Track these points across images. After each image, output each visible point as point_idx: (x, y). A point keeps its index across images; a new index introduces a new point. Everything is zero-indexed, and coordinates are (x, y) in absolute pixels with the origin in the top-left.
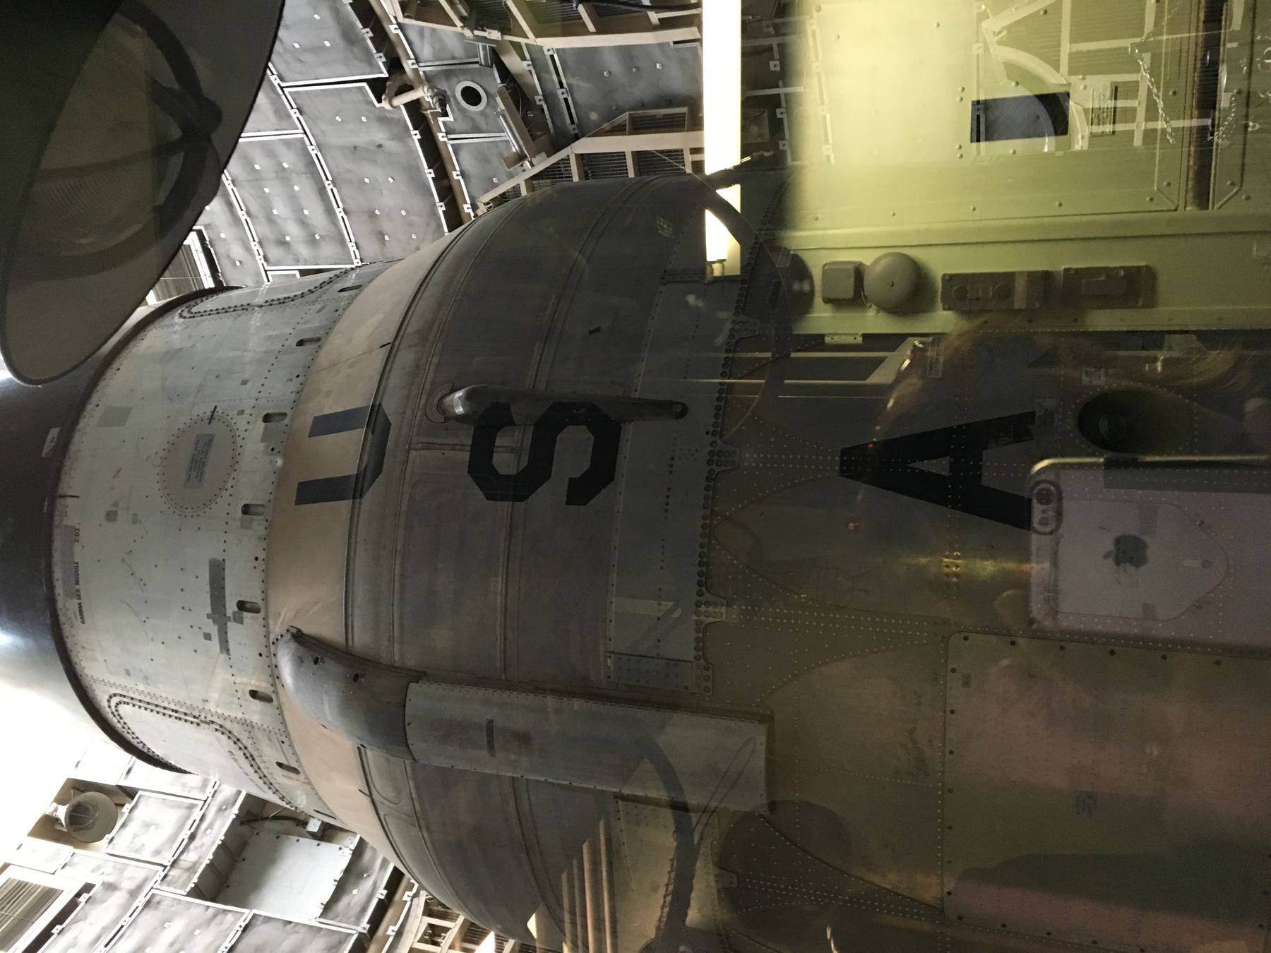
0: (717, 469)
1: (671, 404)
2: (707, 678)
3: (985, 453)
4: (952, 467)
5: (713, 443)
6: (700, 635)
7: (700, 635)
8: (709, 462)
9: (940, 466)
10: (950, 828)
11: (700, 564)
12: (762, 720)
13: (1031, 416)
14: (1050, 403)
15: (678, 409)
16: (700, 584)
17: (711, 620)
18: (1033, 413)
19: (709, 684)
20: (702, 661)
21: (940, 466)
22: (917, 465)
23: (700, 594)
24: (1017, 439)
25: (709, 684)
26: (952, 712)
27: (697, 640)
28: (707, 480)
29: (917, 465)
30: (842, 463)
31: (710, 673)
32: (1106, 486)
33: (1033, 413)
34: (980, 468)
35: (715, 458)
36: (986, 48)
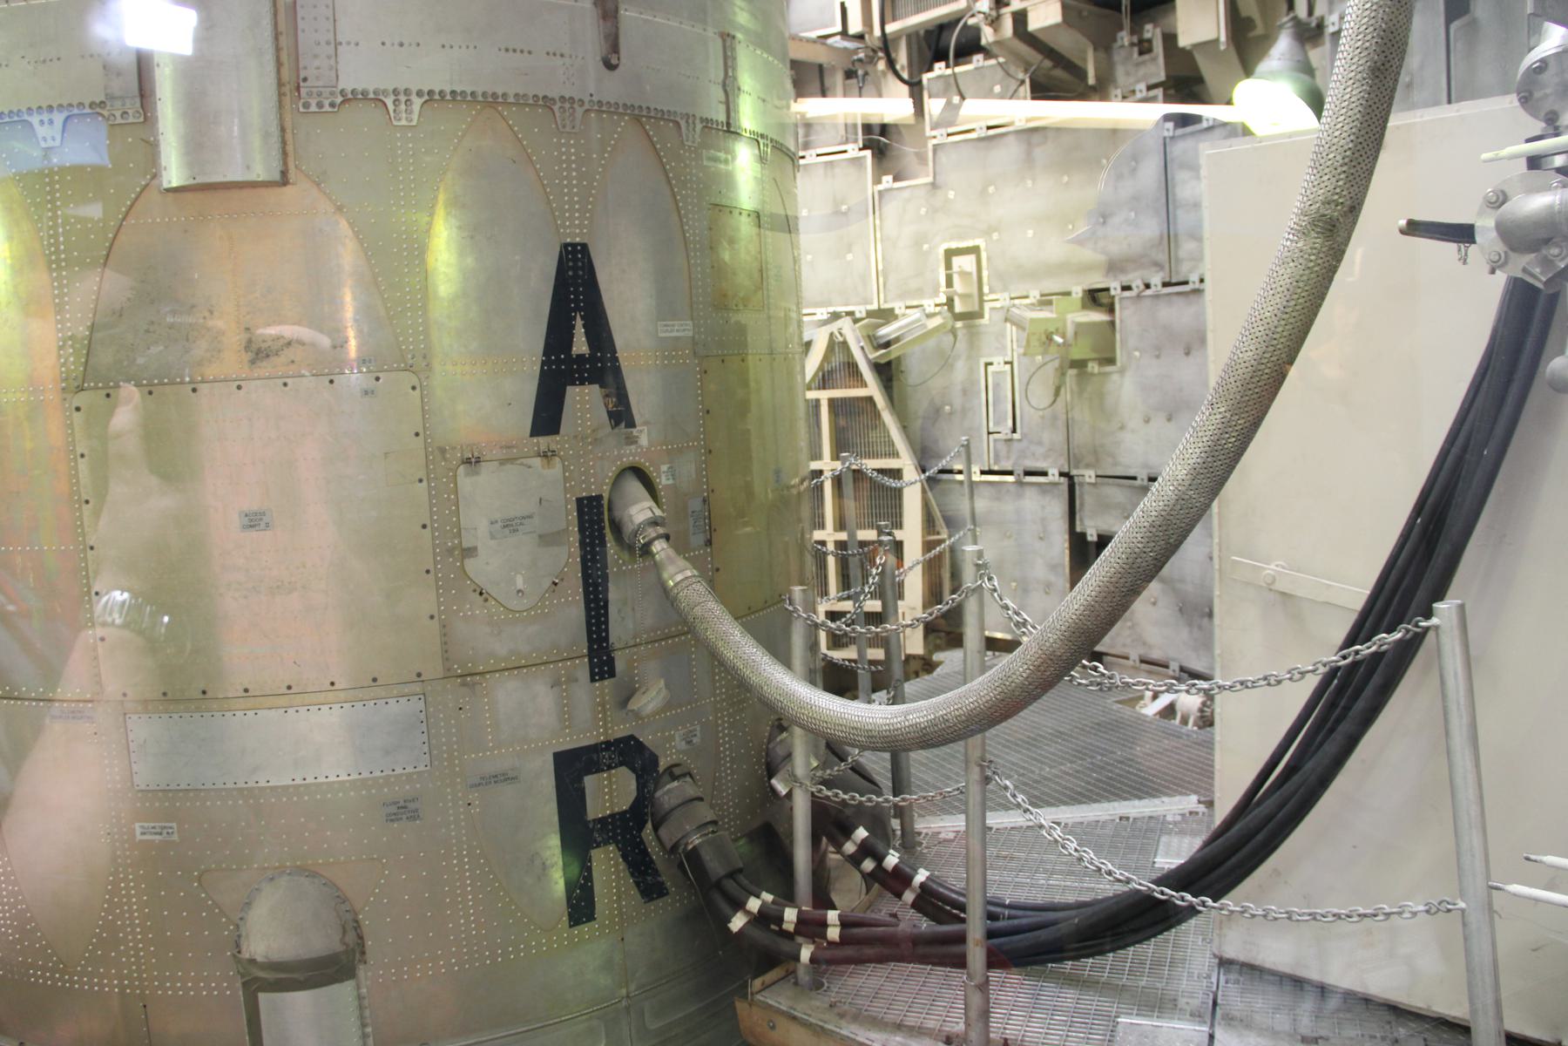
0: (556, 108)
1: (615, 48)
2: (320, 105)
3: (596, 387)
4: (579, 356)
5: (582, 102)
6: (371, 96)
7: (371, 96)
8: (562, 98)
9: (580, 345)
10: (194, 390)
11: (453, 92)
12: (284, 173)
13: (631, 424)
14: (644, 441)
15: (614, 61)
16: (430, 93)
17: (391, 107)
18: (633, 426)
19: (313, 108)
20: (339, 100)
21: (580, 345)
22: (579, 323)
23: (420, 94)
24: (610, 414)
25: (313, 108)
26: (331, 382)
27: (364, 93)
28: (545, 97)
29: (579, 323)
30: (574, 245)
31: (327, 108)
32: (579, 501)
33: (633, 426)
34: (582, 384)
35: (567, 105)
36: (825, 323)
